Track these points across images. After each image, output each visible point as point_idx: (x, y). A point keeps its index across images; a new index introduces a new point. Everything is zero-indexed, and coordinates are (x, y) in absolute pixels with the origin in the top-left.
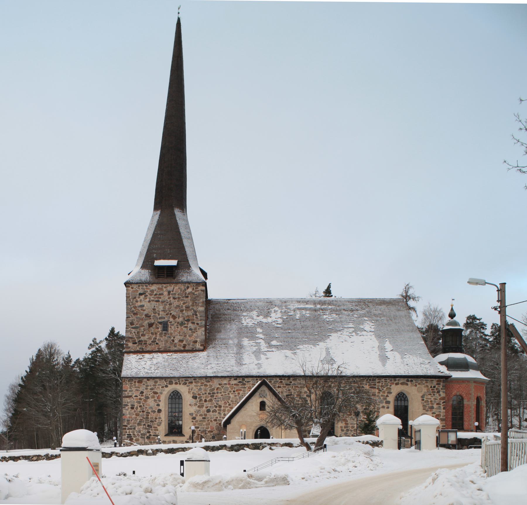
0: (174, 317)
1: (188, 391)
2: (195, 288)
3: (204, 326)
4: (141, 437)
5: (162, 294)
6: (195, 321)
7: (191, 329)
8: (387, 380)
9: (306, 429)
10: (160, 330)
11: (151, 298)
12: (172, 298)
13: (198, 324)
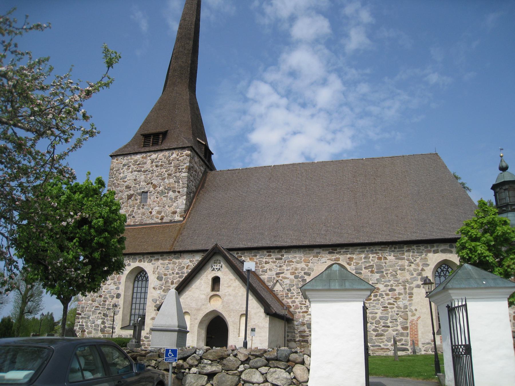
0: (155, 186)
1: (153, 270)
2: (179, 153)
3: (185, 193)
4: (95, 329)
5: (145, 163)
6: (176, 190)
7: (171, 199)
8: (419, 246)
9: (304, 321)
10: (138, 201)
11: (133, 168)
12: (154, 166)
13: (179, 192)
